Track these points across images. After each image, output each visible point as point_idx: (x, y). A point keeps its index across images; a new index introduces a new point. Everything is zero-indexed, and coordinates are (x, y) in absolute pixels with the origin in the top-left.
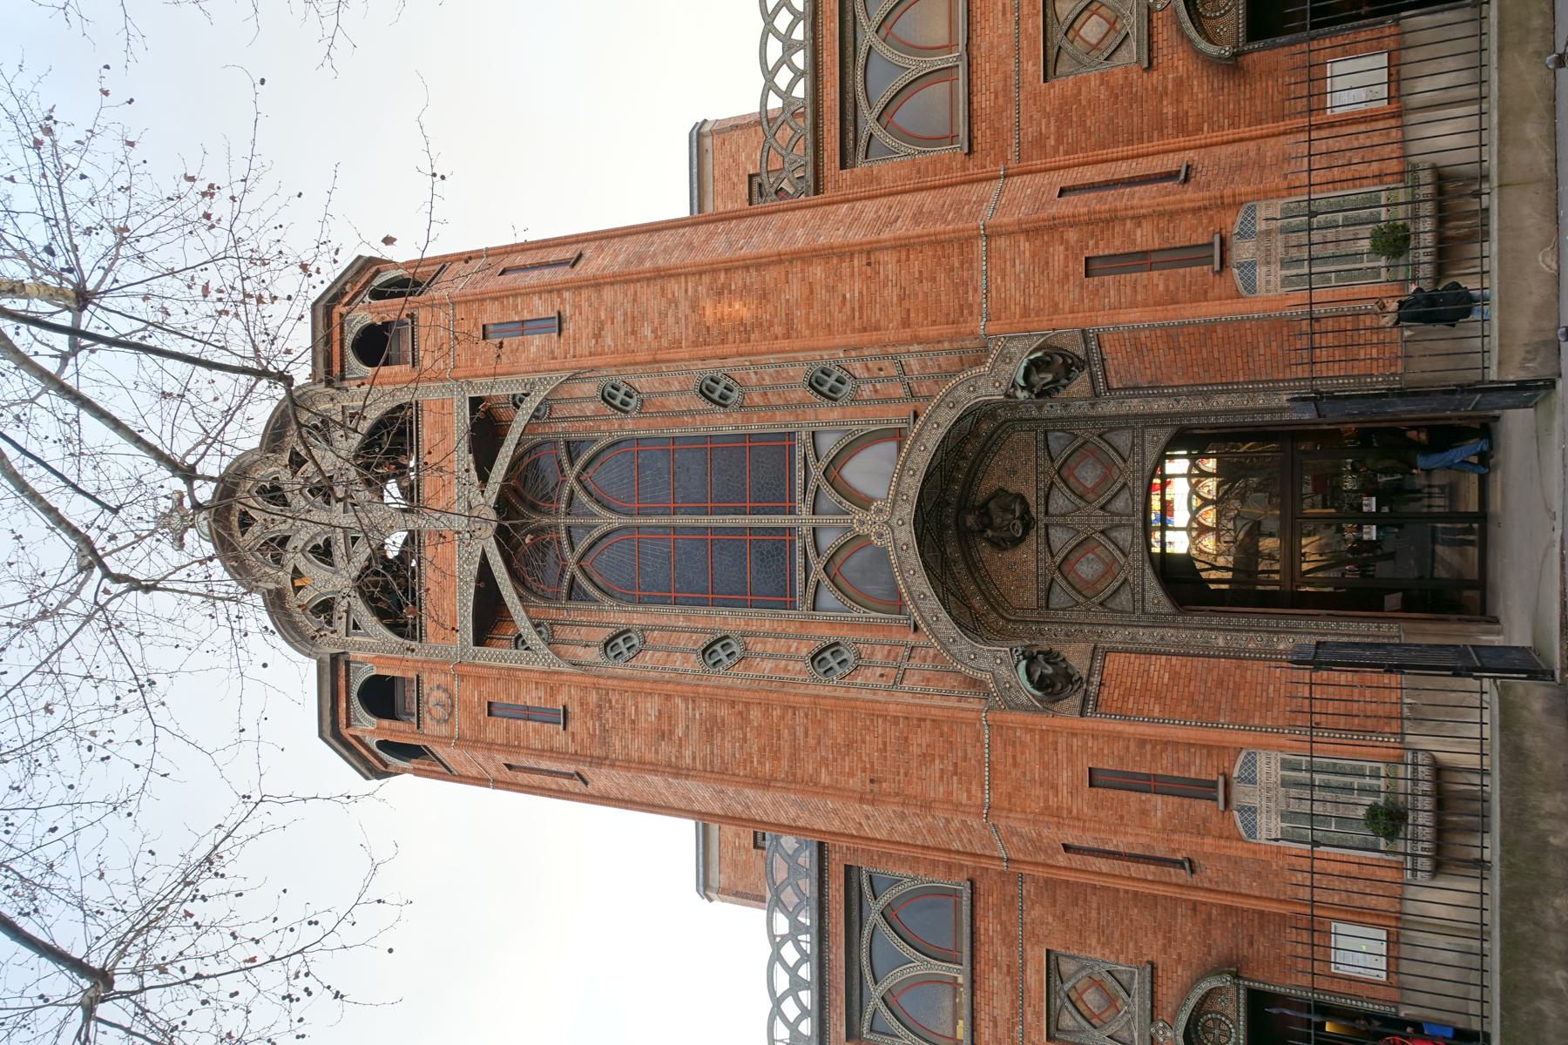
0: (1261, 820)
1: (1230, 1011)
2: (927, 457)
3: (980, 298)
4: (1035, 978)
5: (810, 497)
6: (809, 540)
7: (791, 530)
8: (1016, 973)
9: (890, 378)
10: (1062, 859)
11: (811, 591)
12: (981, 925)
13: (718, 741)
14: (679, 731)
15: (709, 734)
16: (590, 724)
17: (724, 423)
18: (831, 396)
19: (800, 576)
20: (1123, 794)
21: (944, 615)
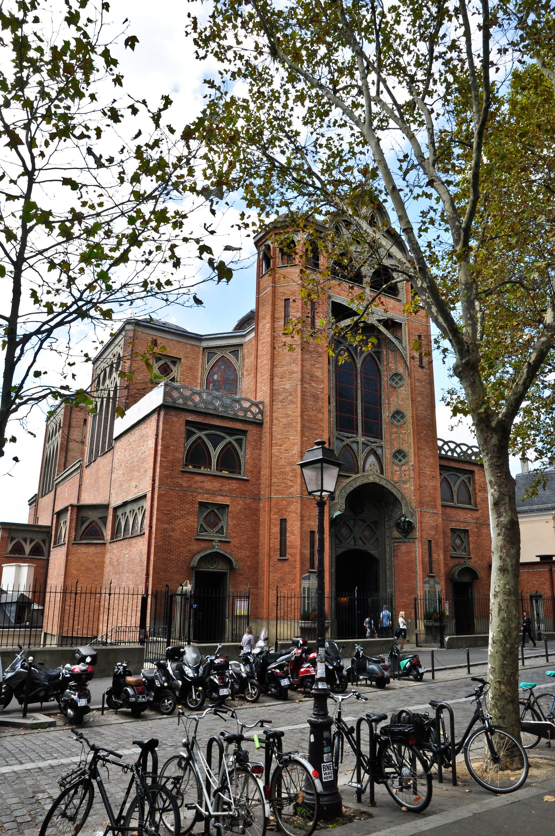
0: (307, 582)
1: (219, 567)
2: (390, 489)
3: (425, 510)
4: (220, 500)
5: (366, 442)
6: (355, 439)
7: (357, 434)
8: (220, 492)
9: (401, 477)
10: (276, 518)
11: (341, 438)
12: (234, 481)
13: (312, 399)
14: (313, 384)
15: (313, 396)
16: (312, 346)
17: (386, 415)
18: (395, 456)
19: (346, 434)
20: (309, 541)
21: (352, 489)
